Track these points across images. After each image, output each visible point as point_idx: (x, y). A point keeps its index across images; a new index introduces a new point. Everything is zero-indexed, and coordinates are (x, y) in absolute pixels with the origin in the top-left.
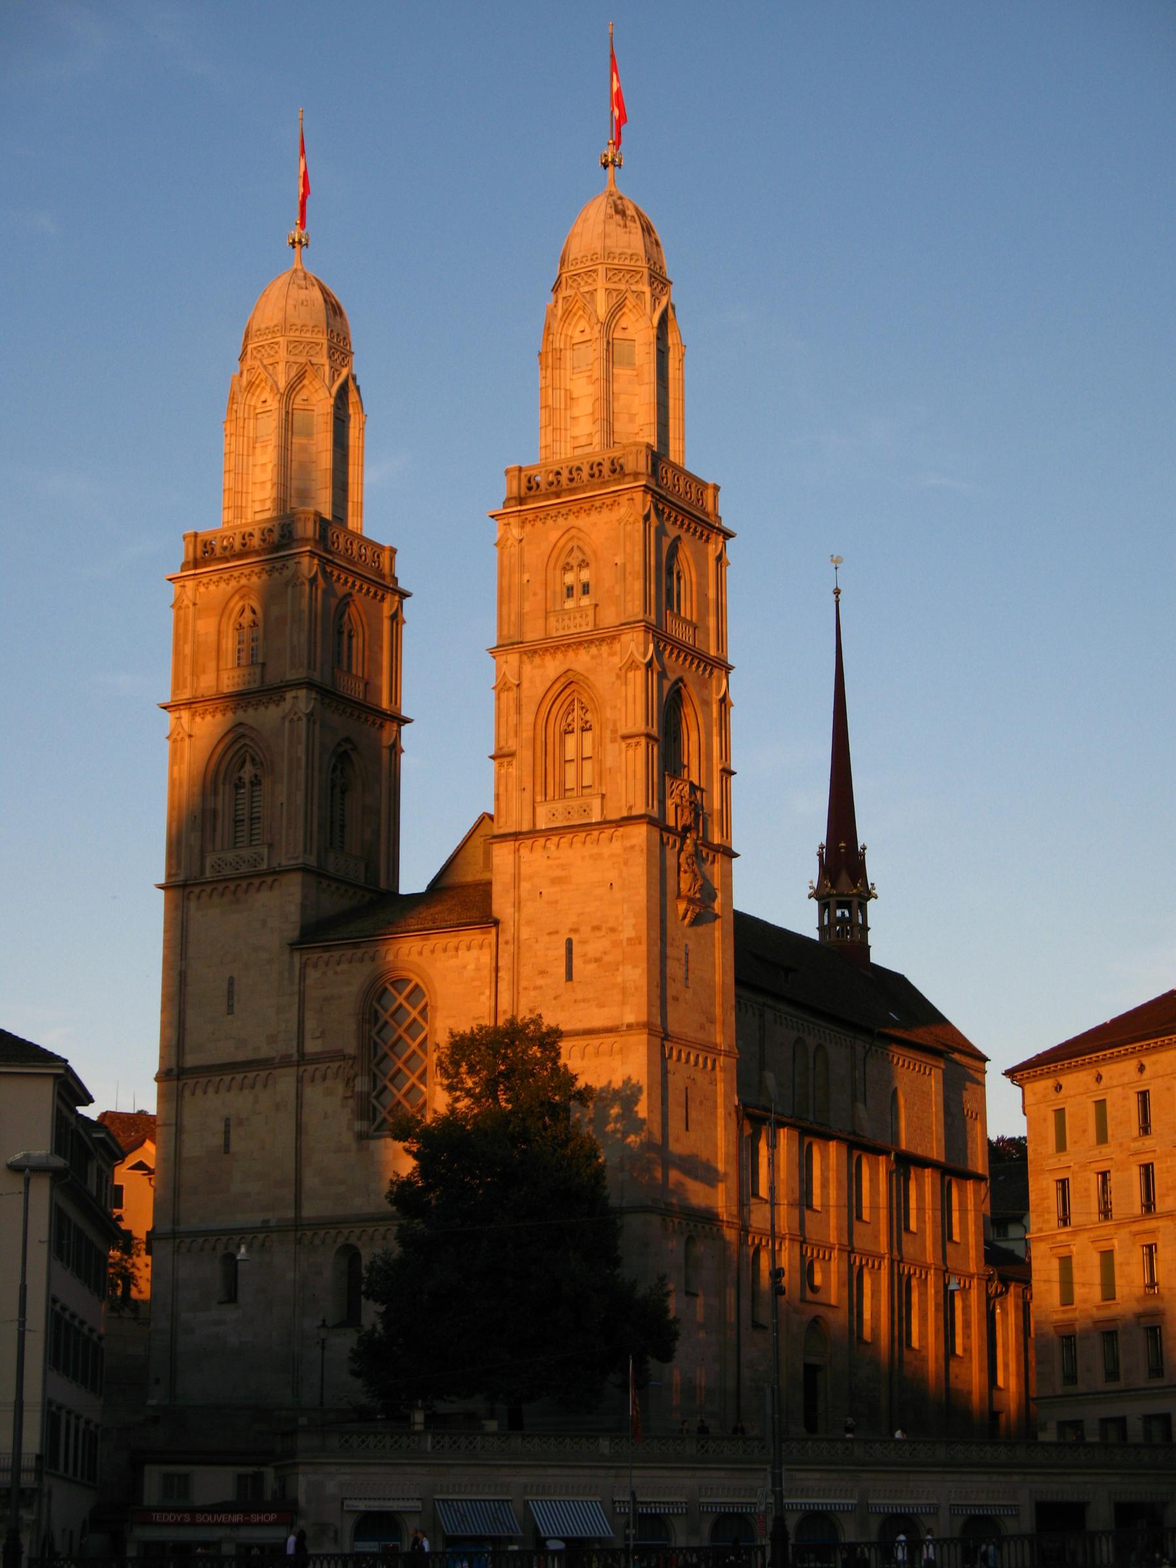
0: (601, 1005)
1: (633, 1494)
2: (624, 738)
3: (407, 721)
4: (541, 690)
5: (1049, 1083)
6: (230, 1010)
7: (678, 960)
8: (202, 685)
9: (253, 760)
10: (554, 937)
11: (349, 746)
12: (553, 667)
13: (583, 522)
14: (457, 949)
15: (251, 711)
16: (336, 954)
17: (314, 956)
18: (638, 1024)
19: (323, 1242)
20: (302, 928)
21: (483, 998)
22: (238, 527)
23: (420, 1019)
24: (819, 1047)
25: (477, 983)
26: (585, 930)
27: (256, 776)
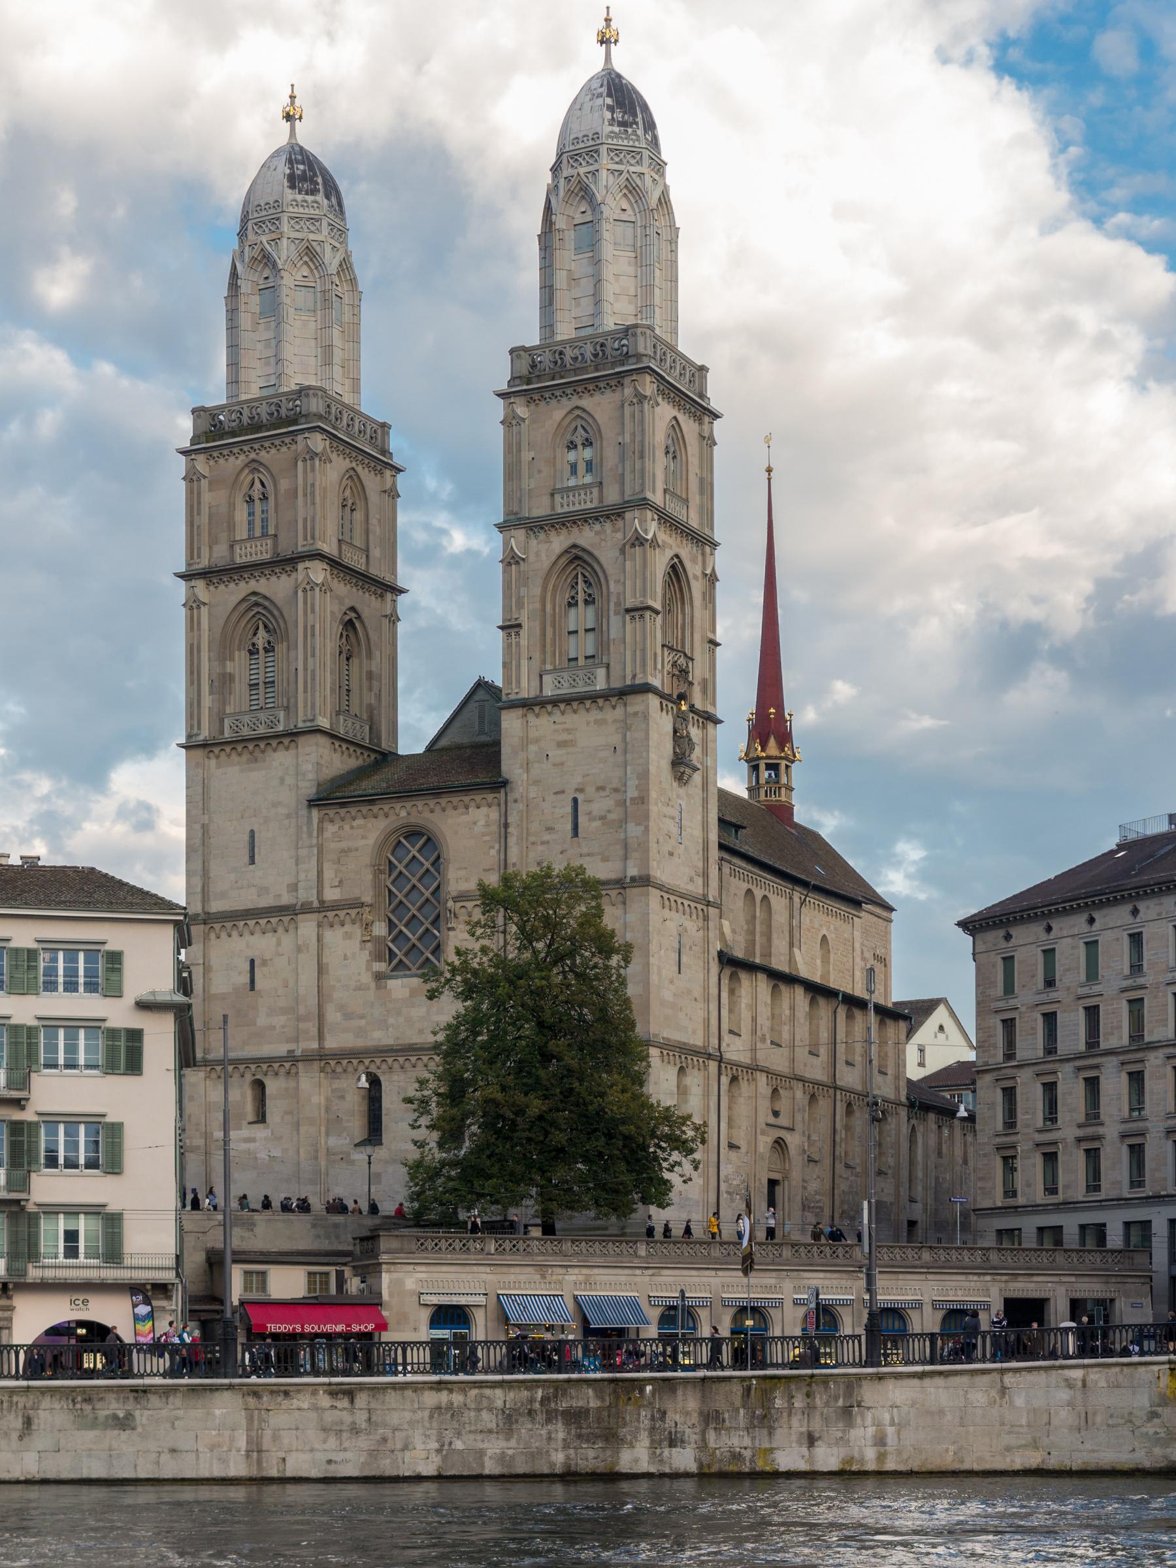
0: (605, 859)
1: (682, 1292)
2: (628, 611)
3: (402, 591)
5: (1001, 933)
7: (673, 818)
9: (266, 627)
10: (560, 796)
11: (353, 615)
14: (467, 807)
15: (263, 581)
17: (331, 813)
19: (345, 1071)
20: (319, 785)
21: (493, 852)
23: (432, 870)
24: (765, 897)
25: (487, 838)
26: (590, 790)
27: (269, 642)
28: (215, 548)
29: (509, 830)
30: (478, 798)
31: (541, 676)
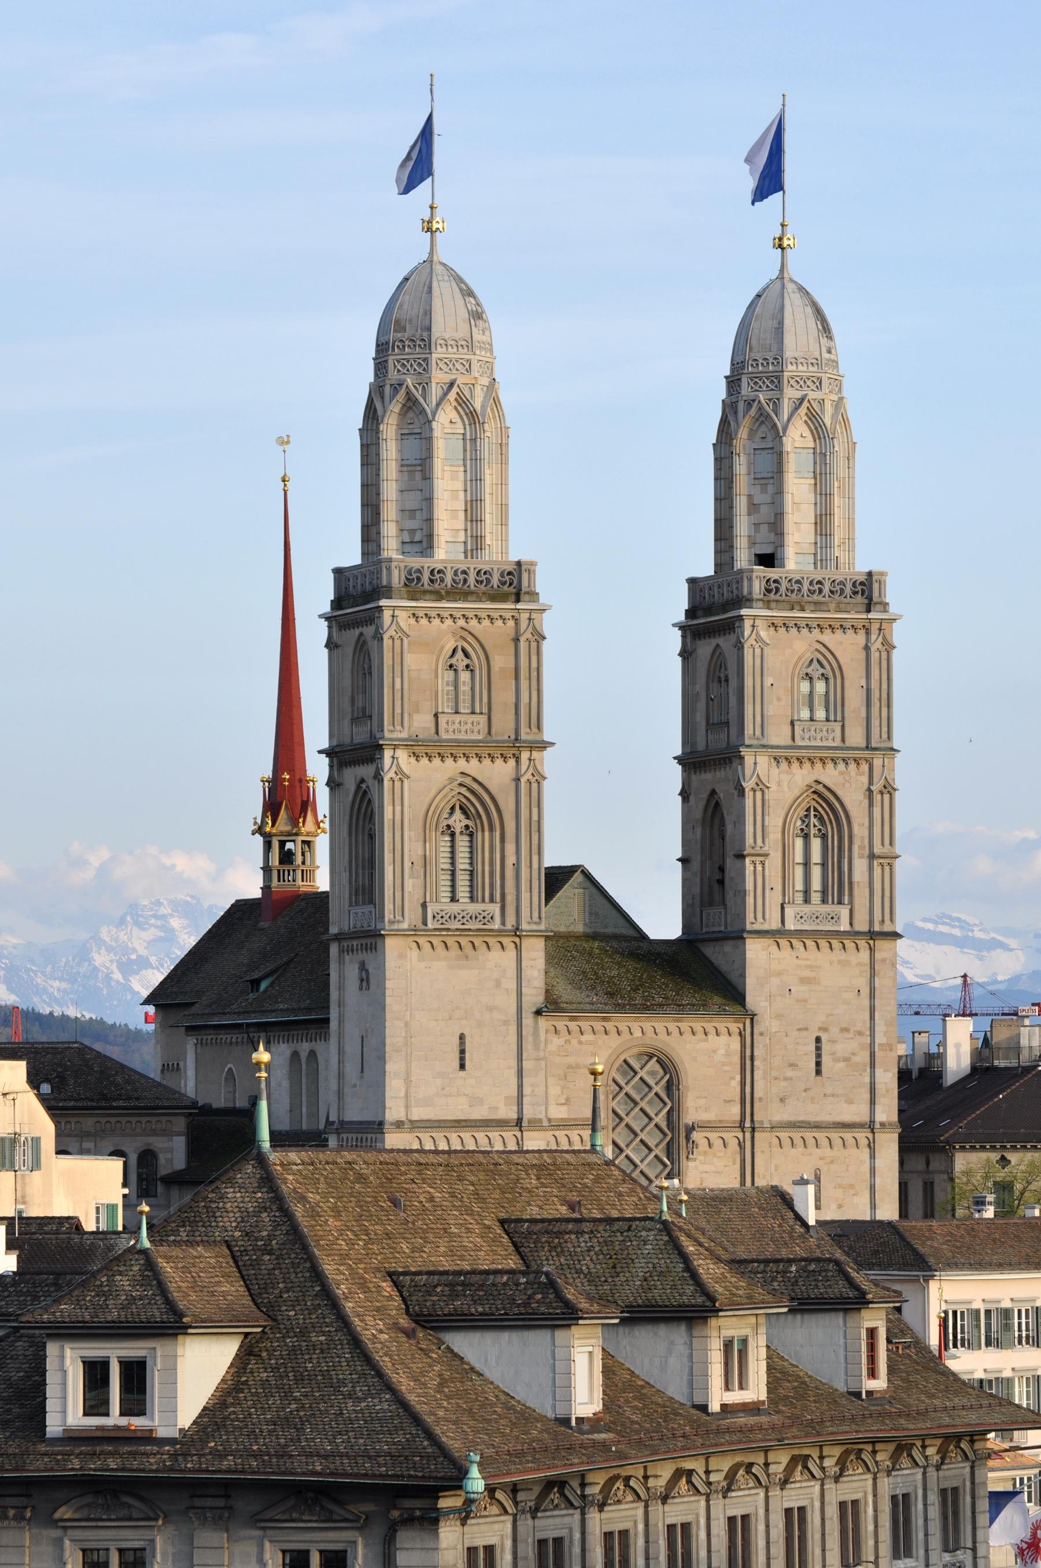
0: (850, 1102)
2: (879, 857)
4: (789, 797)
6: (462, 1067)
8: (416, 724)
9: (461, 808)
10: (804, 1033)
12: (802, 776)
13: (827, 637)
15: (474, 761)
16: (585, 1025)
17: (561, 1025)
18: (890, 1124)
22: (451, 561)
26: (835, 1031)
28: (416, 717)
29: (755, 1063)
30: (722, 1026)
31: (783, 908)
